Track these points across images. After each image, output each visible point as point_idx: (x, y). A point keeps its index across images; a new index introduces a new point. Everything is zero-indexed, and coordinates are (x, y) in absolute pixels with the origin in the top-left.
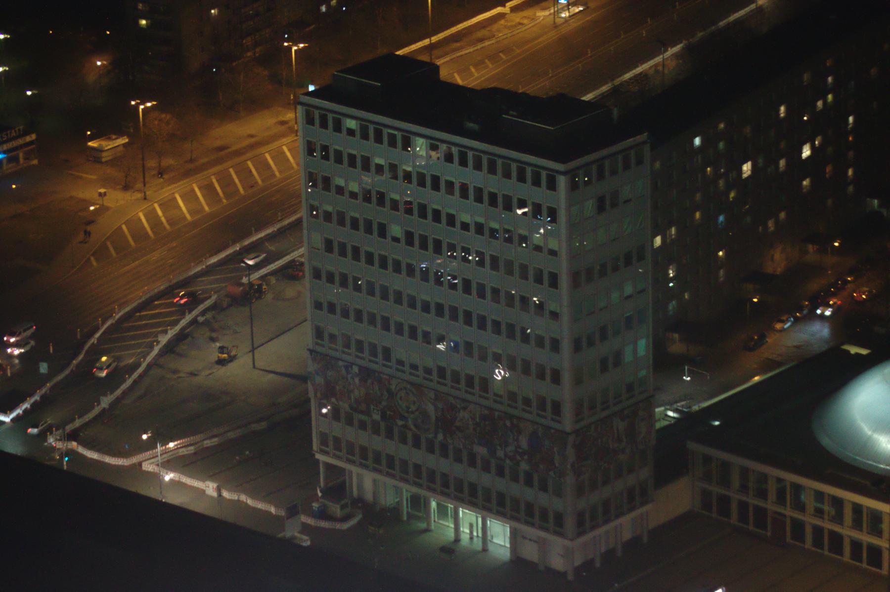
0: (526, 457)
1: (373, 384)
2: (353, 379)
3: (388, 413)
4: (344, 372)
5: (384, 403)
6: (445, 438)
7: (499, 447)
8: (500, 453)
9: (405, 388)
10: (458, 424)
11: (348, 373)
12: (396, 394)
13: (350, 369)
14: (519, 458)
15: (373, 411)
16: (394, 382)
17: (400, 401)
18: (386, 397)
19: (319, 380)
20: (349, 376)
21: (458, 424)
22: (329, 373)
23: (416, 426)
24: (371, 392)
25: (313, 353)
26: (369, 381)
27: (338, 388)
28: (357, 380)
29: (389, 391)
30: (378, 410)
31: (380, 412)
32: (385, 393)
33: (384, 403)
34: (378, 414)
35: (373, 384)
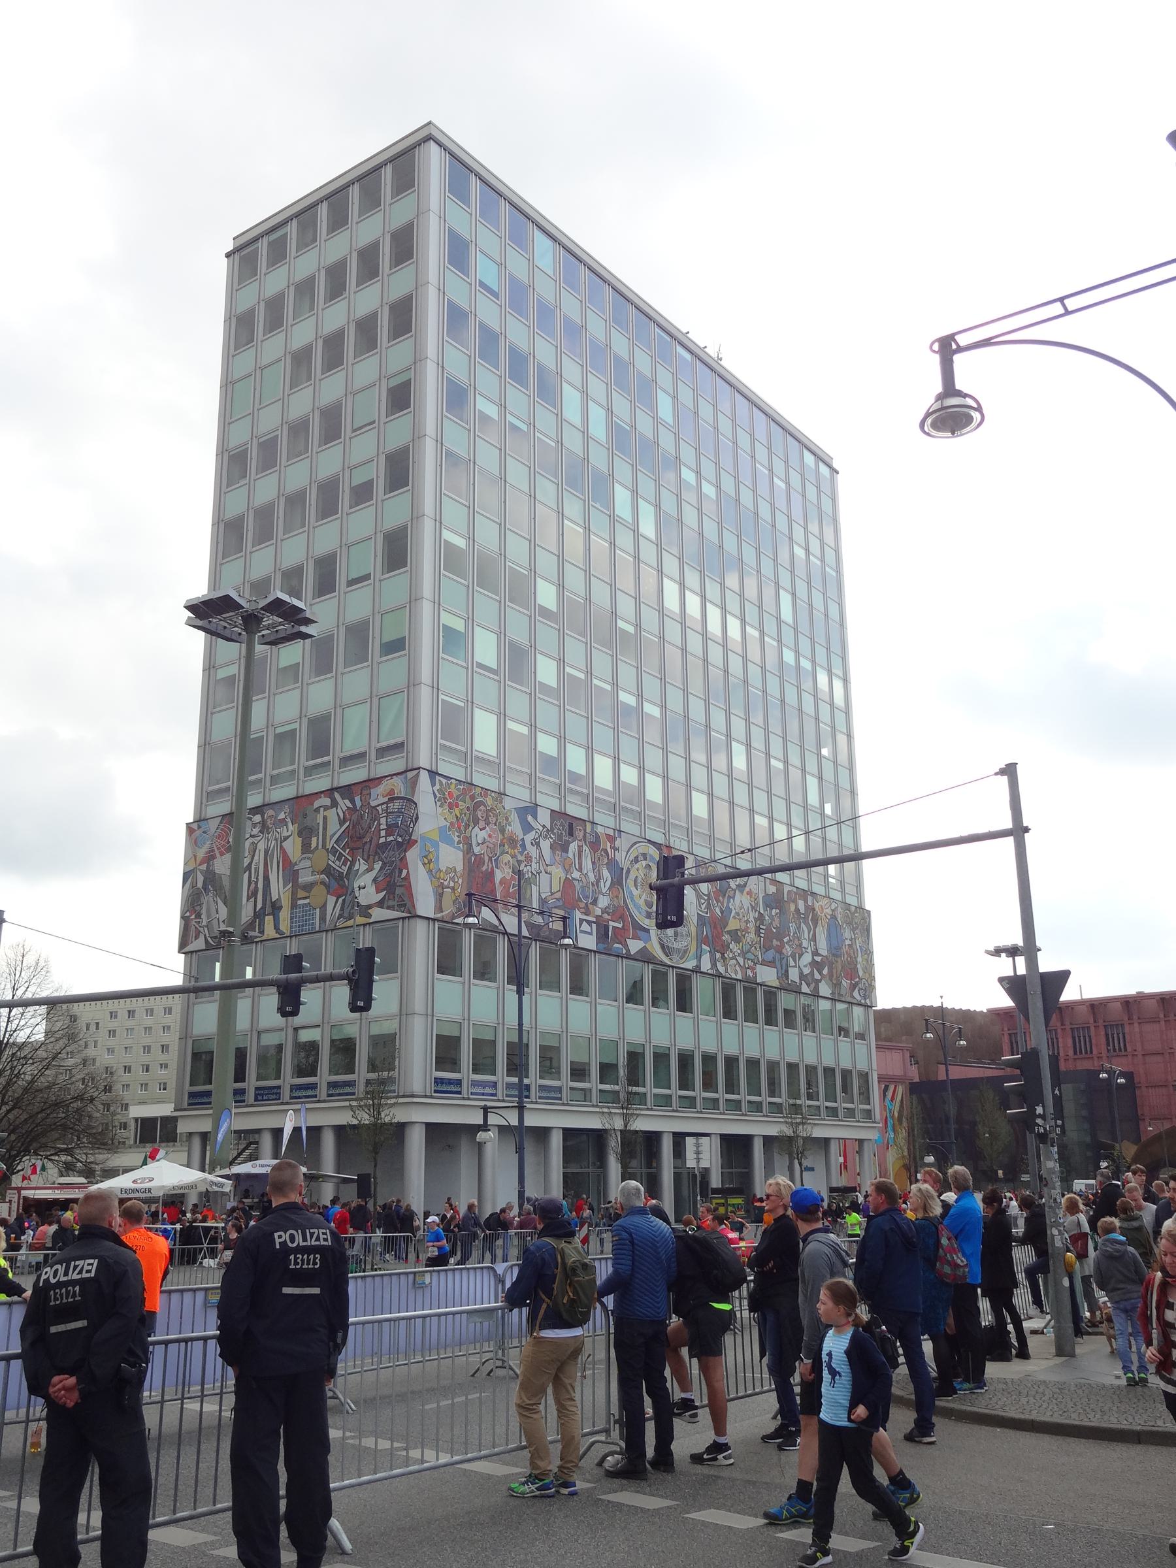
0: (825, 972)
1: (580, 852)
2: (538, 844)
3: (611, 924)
4: (515, 828)
5: (603, 902)
6: (714, 965)
7: (792, 963)
8: (794, 975)
9: (644, 856)
10: (733, 925)
11: (528, 828)
12: (628, 871)
13: (530, 818)
14: (817, 976)
15: (580, 925)
16: (622, 843)
17: (633, 889)
18: (608, 883)
19: (451, 858)
20: (529, 838)
21: (733, 925)
22: (479, 835)
23: (663, 947)
24: (576, 875)
25: (438, 778)
26: (573, 847)
27: (498, 875)
28: (545, 845)
29: (612, 864)
30: (589, 923)
31: (594, 926)
32: (606, 874)
33: (603, 902)
34: (590, 933)
35: (580, 852)
